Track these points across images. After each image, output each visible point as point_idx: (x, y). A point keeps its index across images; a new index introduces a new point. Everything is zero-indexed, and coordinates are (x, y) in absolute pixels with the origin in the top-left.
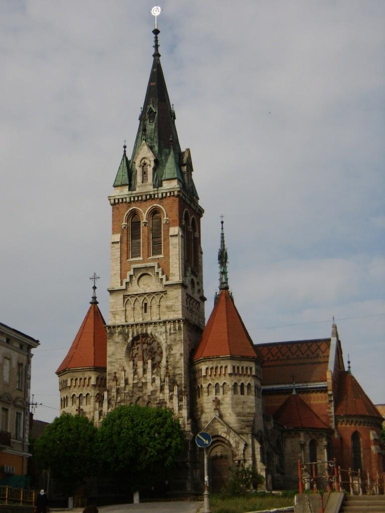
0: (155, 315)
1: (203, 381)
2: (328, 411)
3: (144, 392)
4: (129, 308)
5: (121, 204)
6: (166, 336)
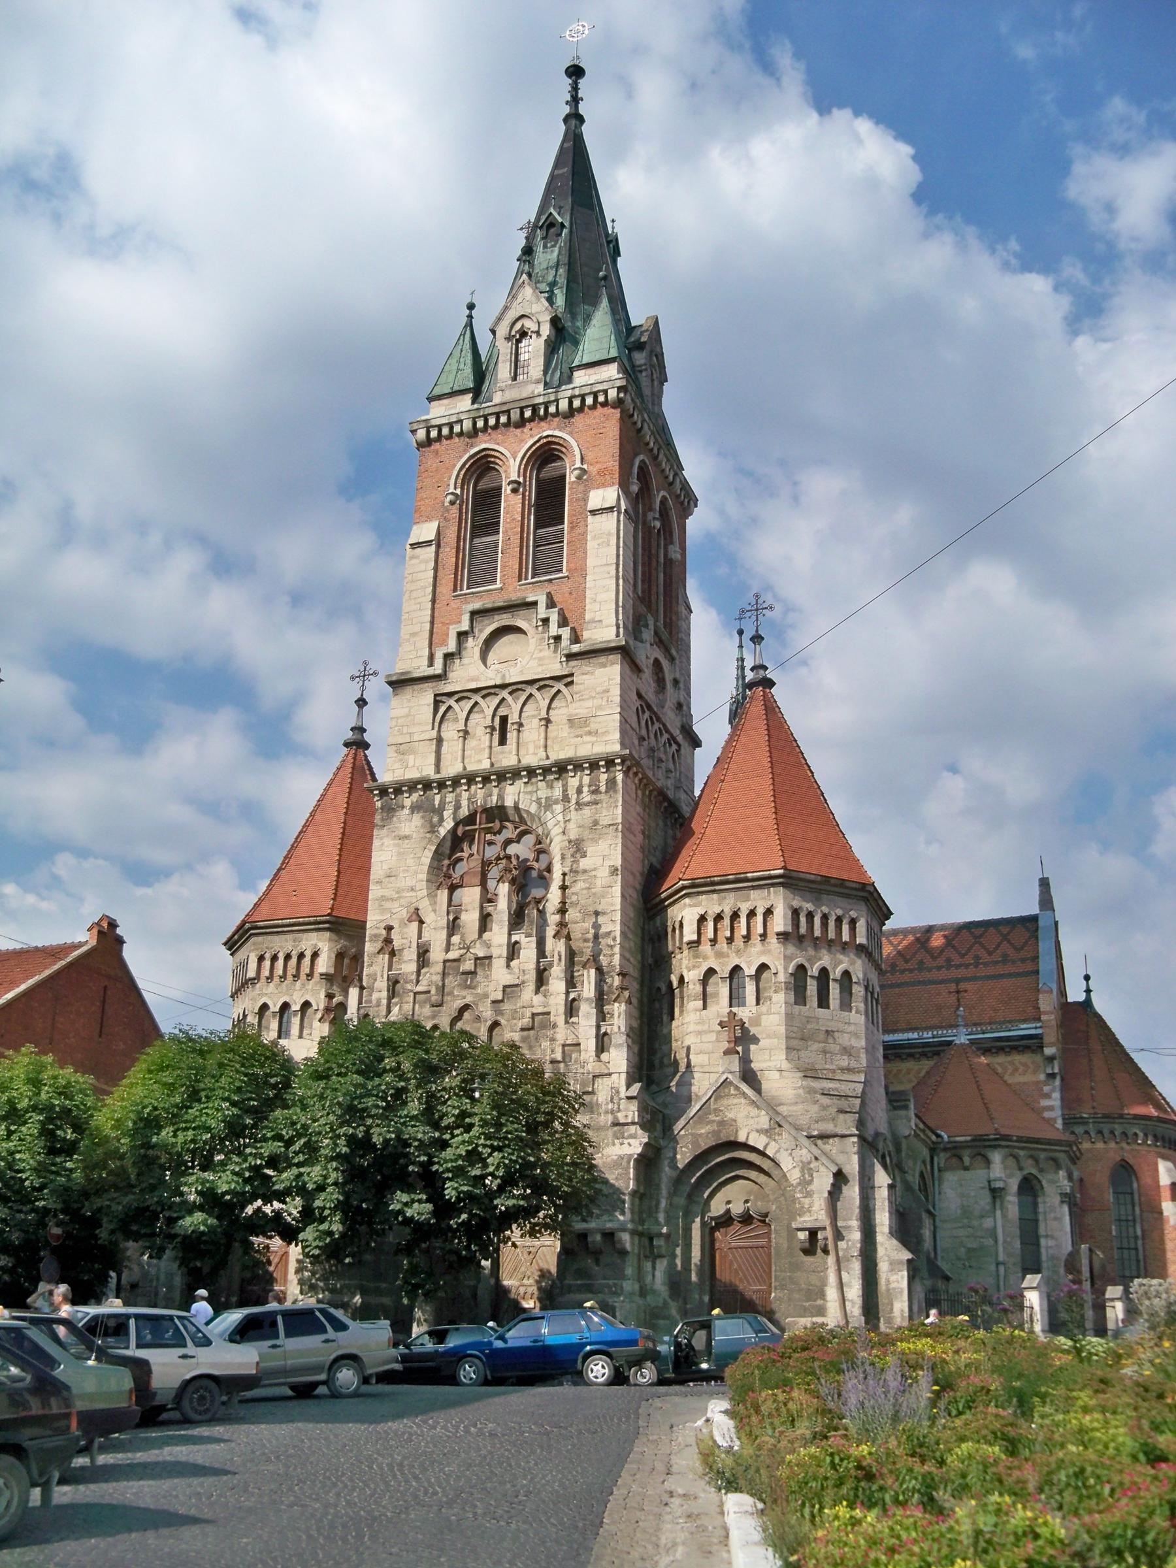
1: (685, 962)
2: (1045, 1103)
3: (479, 990)
4: (450, 732)
5: (445, 442)
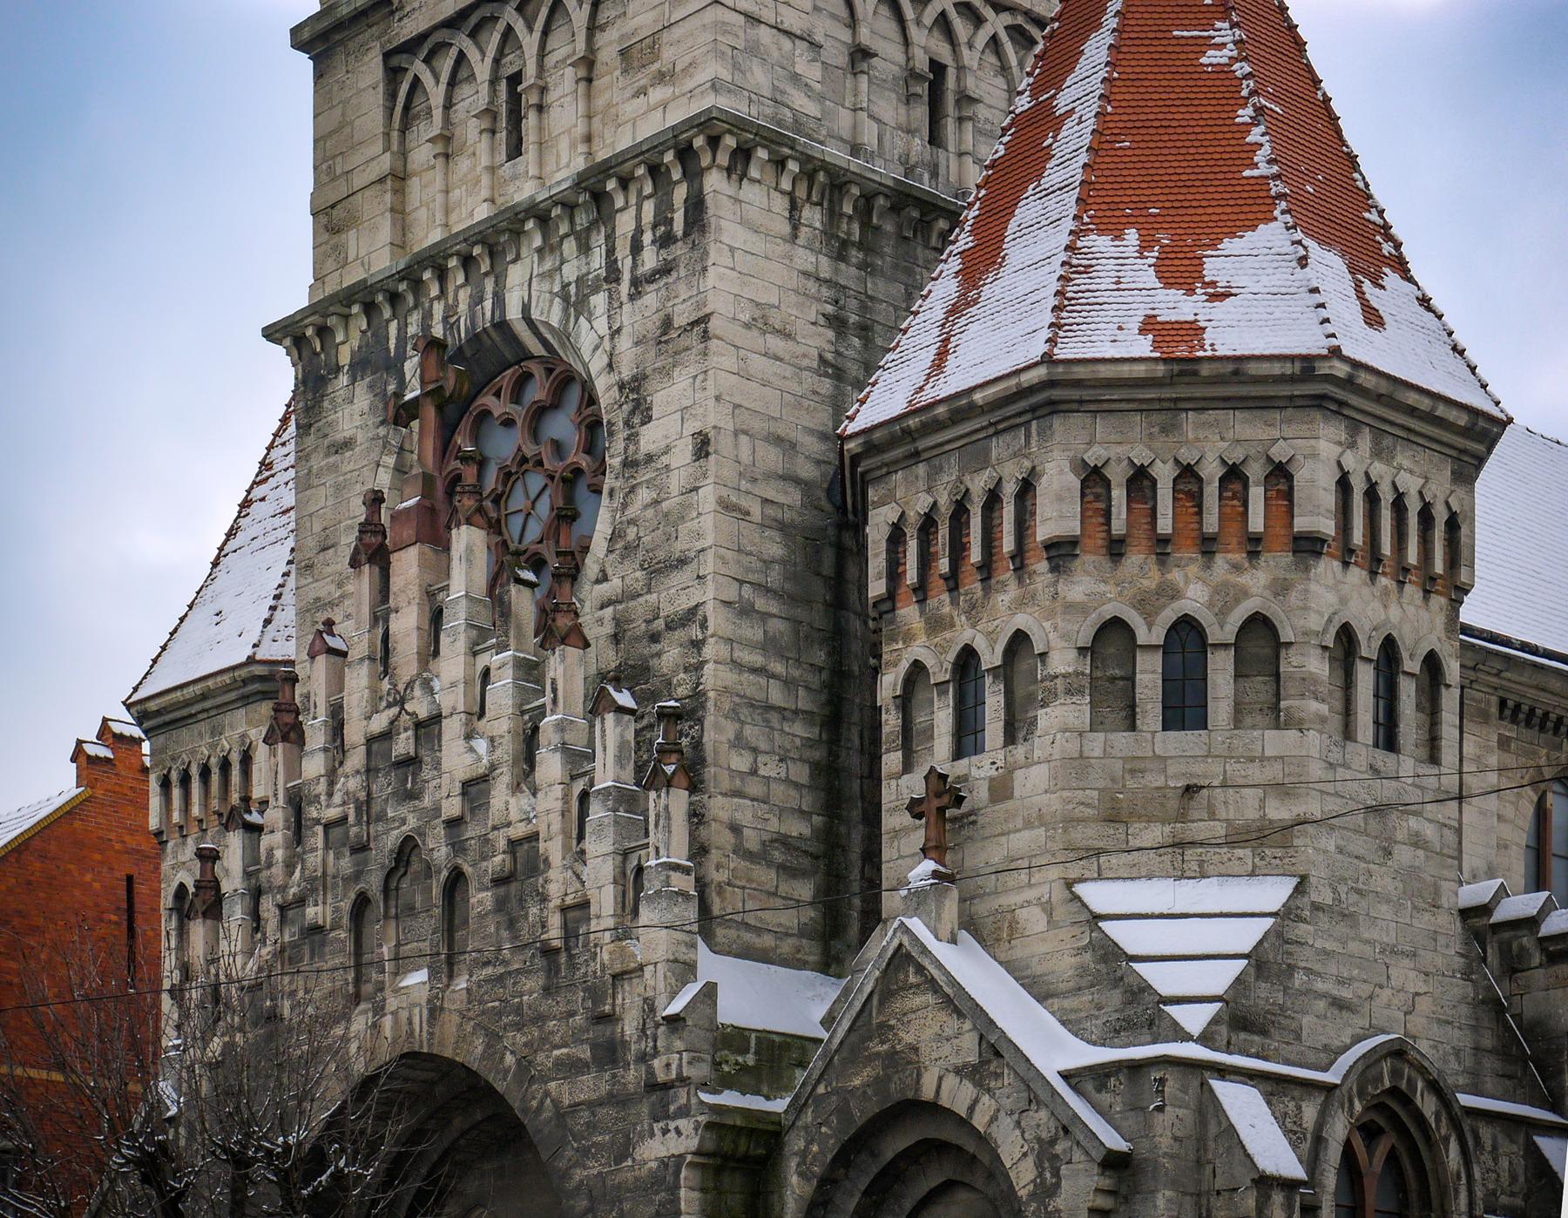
0: (564, 144)
3: (427, 801)
6: (614, 306)
